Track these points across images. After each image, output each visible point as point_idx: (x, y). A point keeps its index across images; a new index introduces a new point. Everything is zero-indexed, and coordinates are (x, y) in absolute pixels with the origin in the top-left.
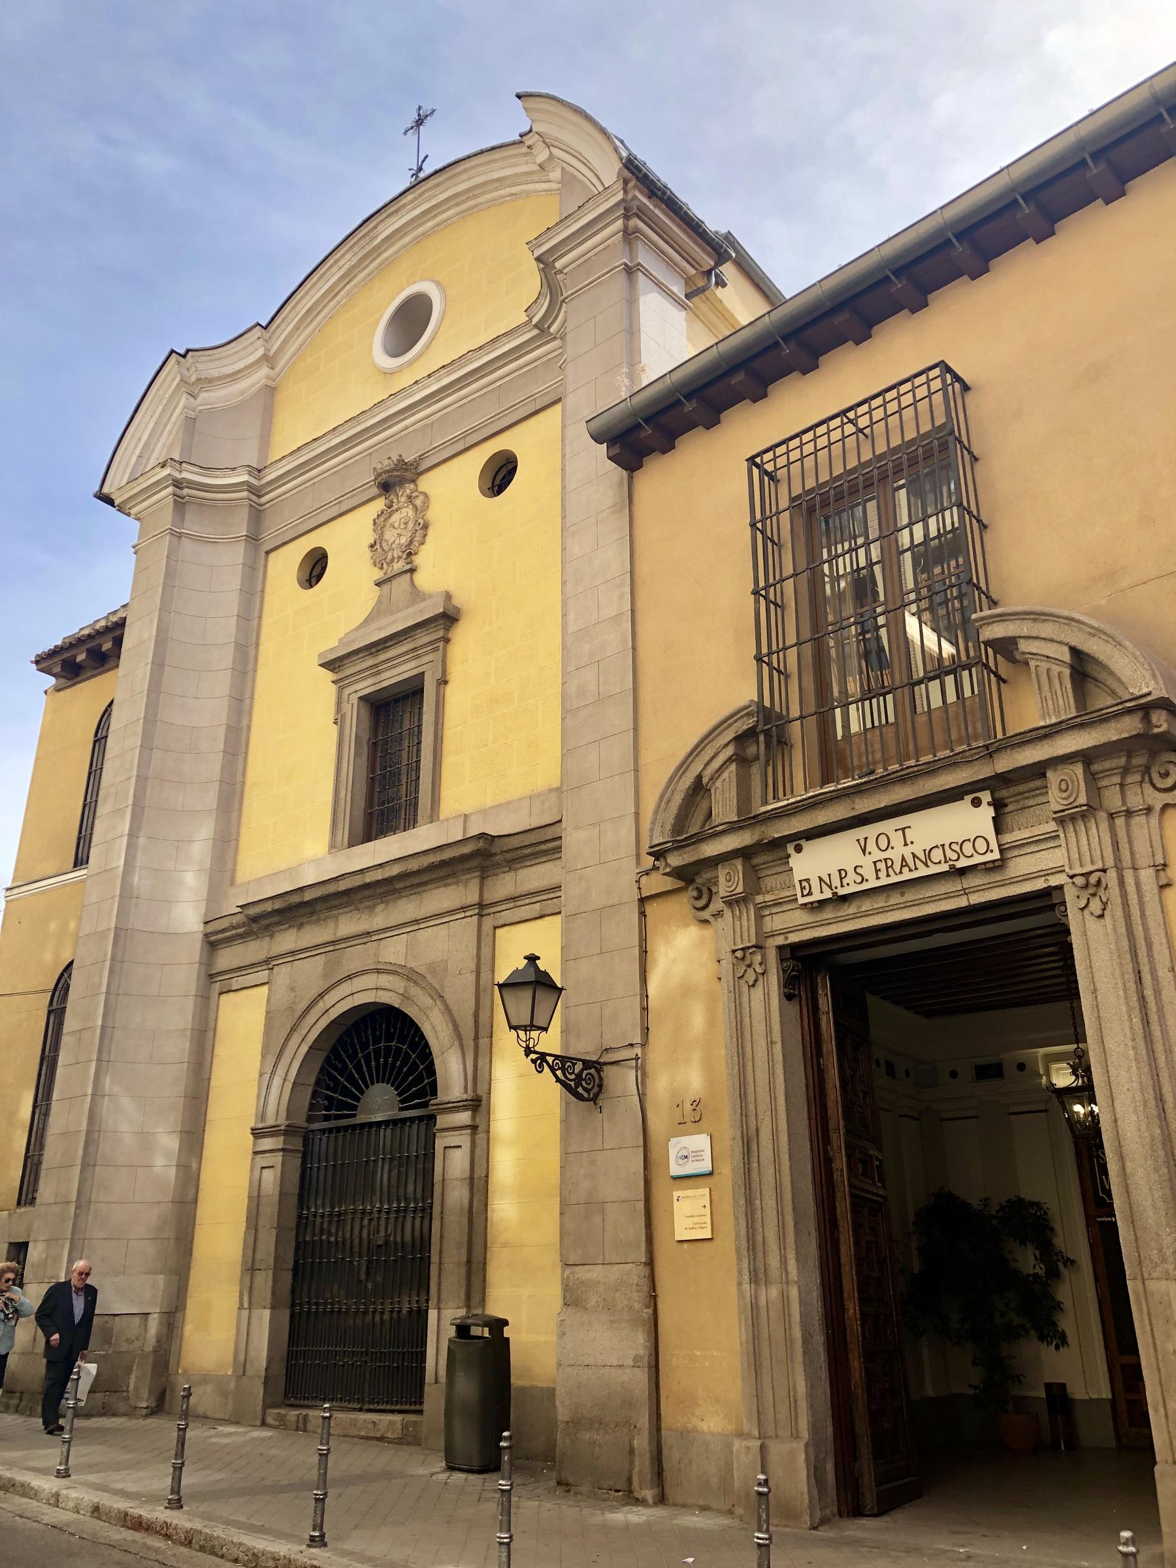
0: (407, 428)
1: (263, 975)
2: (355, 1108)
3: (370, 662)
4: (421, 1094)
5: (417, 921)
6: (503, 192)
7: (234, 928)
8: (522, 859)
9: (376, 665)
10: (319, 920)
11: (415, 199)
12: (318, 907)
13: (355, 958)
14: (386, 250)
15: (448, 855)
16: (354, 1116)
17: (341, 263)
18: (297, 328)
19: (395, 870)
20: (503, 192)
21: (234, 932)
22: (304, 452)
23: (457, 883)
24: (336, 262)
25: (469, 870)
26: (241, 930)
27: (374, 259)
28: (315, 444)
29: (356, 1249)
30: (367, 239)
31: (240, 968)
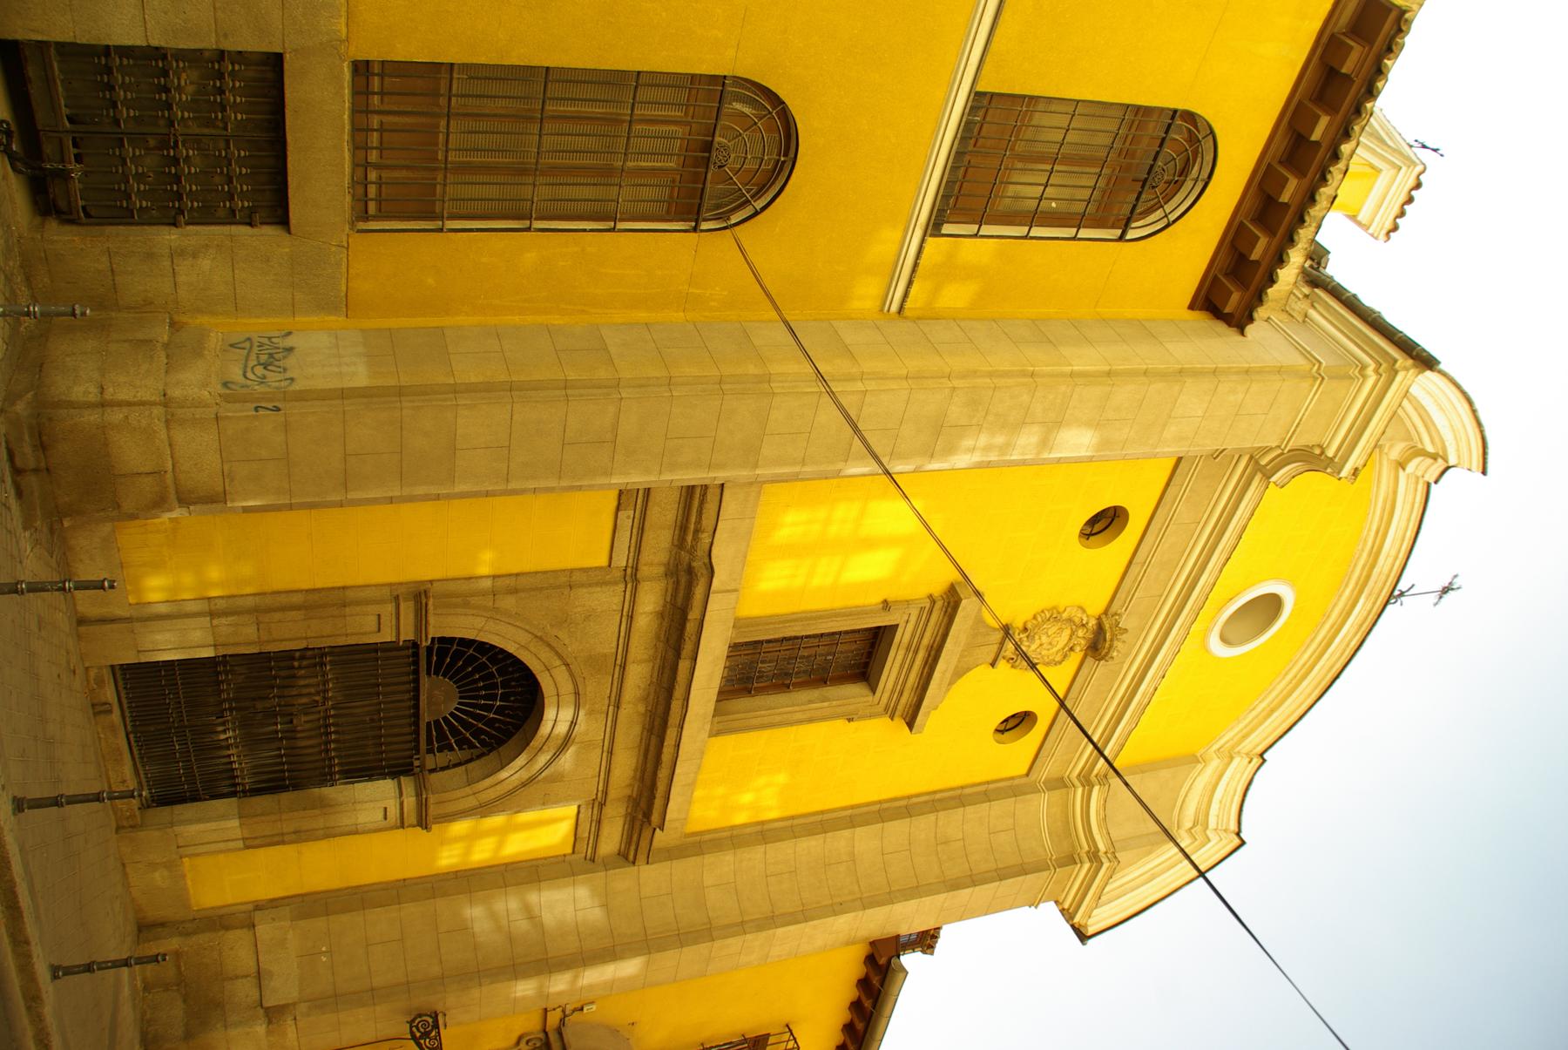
1: (621, 560)
2: (437, 673)
3: (925, 641)
4: (442, 736)
5: (611, 752)
7: (697, 531)
8: (632, 828)
9: (916, 652)
10: (658, 638)
12: (671, 654)
13: (598, 689)
15: (658, 802)
16: (429, 674)
17: (1390, 560)
18: (1395, 492)
19: (666, 756)
21: (692, 527)
22: (1235, 536)
23: (634, 777)
25: (640, 794)
26: (689, 538)
28: (1224, 557)
29: (286, 692)
30: (1376, 591)
31: (642, 530)
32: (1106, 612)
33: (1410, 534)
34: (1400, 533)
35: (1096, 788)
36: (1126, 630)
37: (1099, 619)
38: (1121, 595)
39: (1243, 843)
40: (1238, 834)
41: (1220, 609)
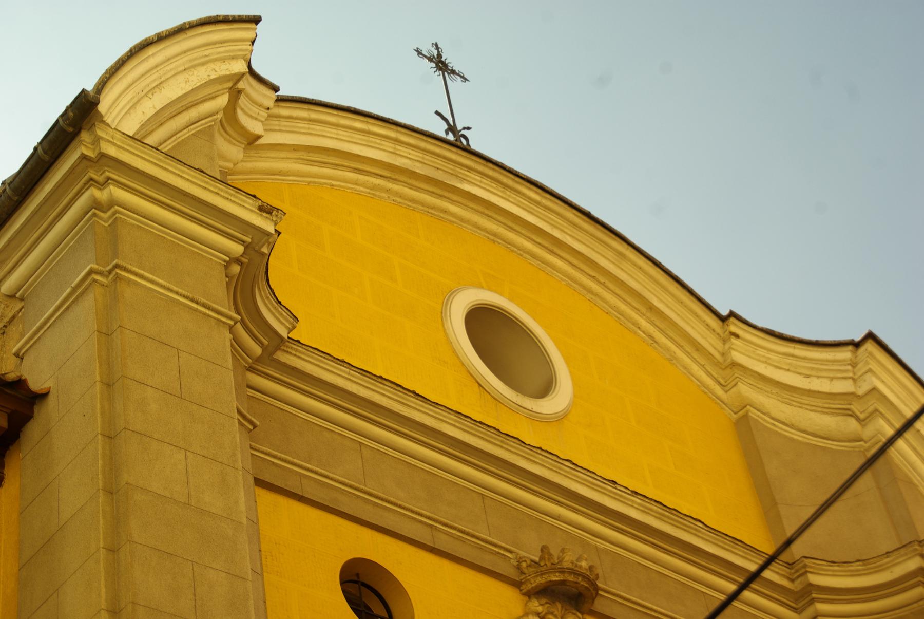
0: (558, 518)
6: (643, 323)
11: (538, 203)
14: (453, 202)
17: (401, 150)
18: (295, 148)
20: (643, 323)
22: (379, 387)
24: (397, 141)
27: (432, 193)
28: (413, 401)
30: (450, 167)
32: (516, 584)
33: (359, 123)
34: (358, 137)
35: (814, 579)
36: (544, 549)
37: (529, 595)
38: (487, 561)
39: (870, 336)
40: (857, 345)
41: (497, 400)
